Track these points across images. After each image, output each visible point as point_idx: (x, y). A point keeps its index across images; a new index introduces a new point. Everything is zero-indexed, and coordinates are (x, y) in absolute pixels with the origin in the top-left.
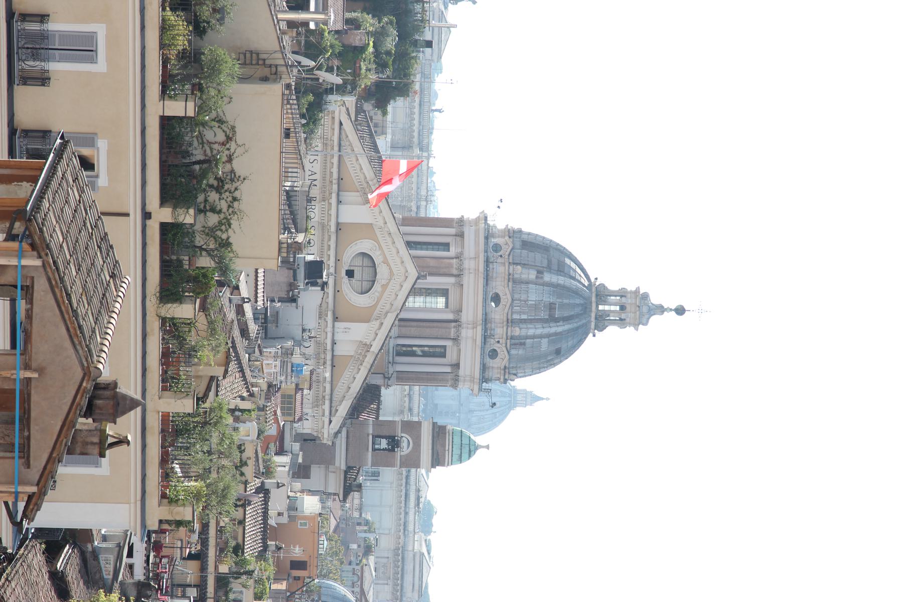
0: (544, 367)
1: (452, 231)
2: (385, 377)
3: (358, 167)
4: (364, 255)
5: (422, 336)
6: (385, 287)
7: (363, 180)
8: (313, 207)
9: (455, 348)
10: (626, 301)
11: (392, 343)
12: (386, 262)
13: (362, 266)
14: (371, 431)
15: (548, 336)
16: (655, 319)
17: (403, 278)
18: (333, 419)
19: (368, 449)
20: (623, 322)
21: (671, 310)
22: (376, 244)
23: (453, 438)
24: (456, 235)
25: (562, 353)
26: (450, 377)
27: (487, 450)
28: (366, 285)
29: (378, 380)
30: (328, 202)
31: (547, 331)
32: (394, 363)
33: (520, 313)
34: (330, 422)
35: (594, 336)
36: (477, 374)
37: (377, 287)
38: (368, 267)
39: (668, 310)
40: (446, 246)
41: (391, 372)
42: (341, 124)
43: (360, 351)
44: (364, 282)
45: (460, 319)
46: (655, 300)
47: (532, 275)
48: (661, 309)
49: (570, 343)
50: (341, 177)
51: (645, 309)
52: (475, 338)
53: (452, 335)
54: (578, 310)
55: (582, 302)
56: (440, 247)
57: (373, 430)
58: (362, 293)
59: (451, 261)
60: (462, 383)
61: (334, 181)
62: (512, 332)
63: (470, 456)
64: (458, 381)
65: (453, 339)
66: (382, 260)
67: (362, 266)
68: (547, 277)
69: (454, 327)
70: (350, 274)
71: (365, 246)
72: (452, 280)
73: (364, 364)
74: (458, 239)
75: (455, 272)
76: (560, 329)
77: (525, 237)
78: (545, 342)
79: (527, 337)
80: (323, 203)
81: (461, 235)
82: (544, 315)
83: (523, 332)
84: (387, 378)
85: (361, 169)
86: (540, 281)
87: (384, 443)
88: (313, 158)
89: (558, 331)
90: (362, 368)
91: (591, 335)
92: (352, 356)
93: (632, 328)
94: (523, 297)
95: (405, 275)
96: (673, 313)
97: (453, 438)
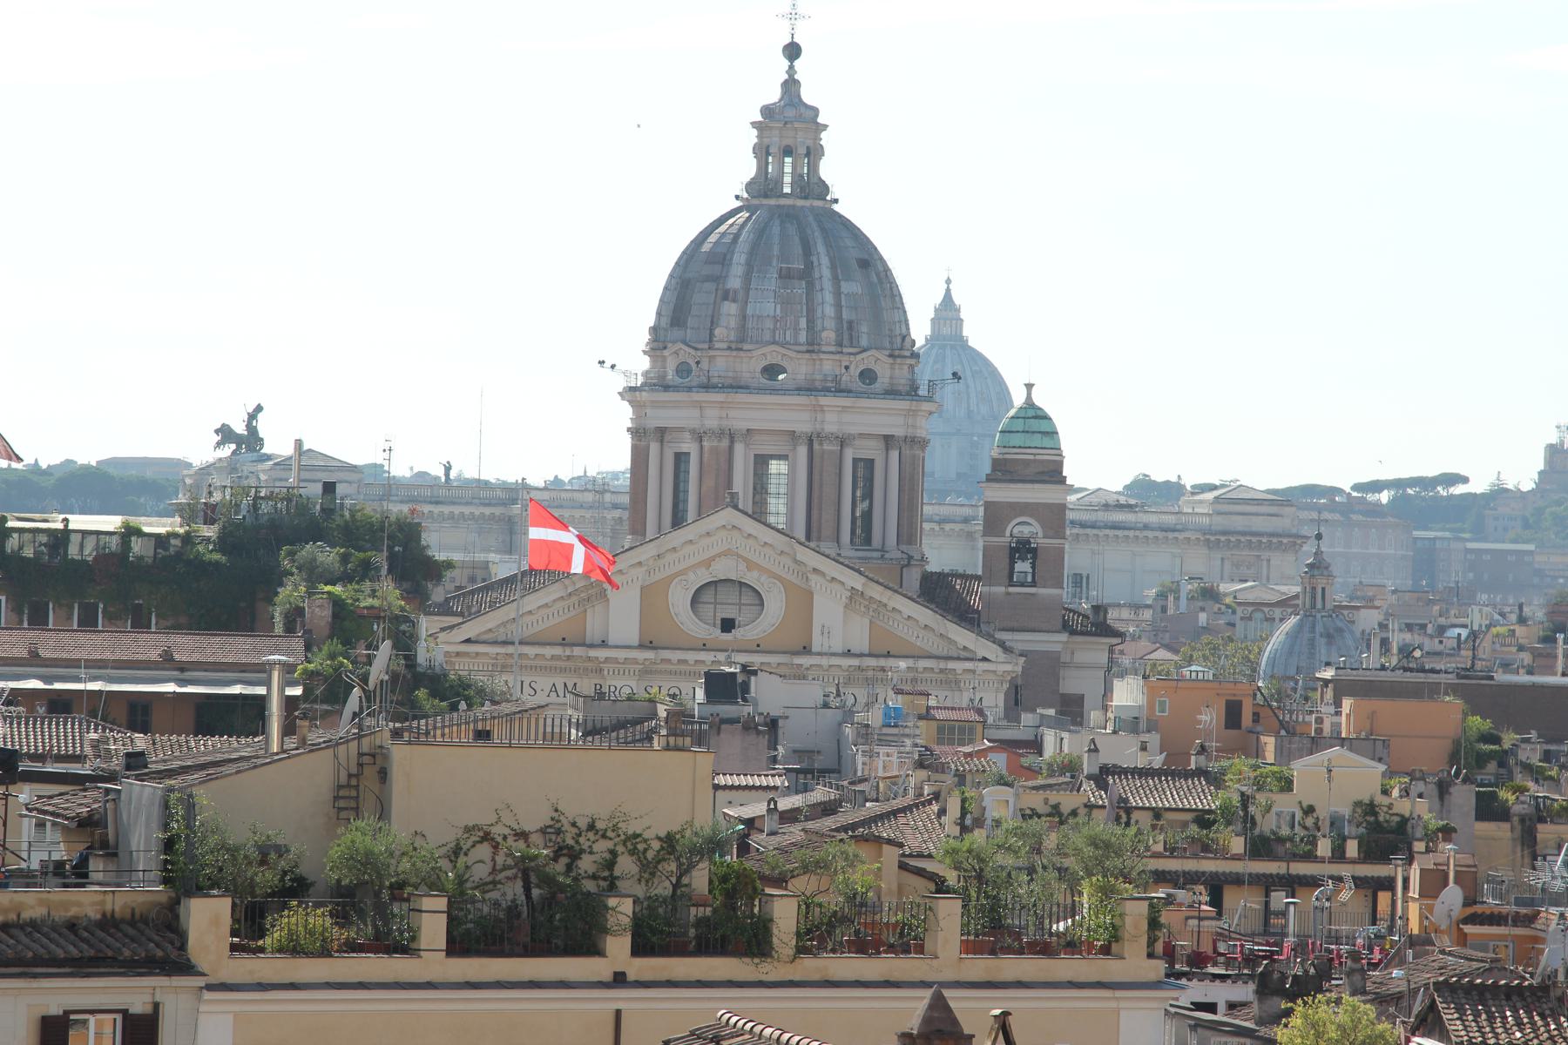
0: (891, 288)
1: (654, 448)
2: (908, 565)
3: (544, 612)
4: (695, 600)
6: (751, 565)
8: (612, 689)
9: (857, 442)
10: (776, 143)
11: (848, 552)
12: (707, 563)
13: (716, 603)
14: (1002, 589)
15: (836, 279)
16: (808, 96)
17: (735, 533)
18: (980, 654)
21: (791, 67)
22: (676, 580)
23: (1014, 447)
24: (662, 442)
25: (866, 257)
26: (907, 452)
27: (1034, 389)
28: (747, 598)
29: (913, 578)
30: (604, 663)
31: (827, 284)
32: (883, 550)
33: (796, 330)
34: (985, 659)
35: (836, 201)
37: (751, 578)
38: (716, 594)
39: (791, 72)
40: (680, 459)
41: (899, 555)
42: (468, 641)
43: (863, 609)
46: (773, 95)
47: (730, 308)
48: (791, 85)
49: (849, 242)
51: (790, 113)
52: (840, 409)
54: (792, 230)
55: (777, 222)
56: (682, 469)
57: (1000, 585)
58: (762, 604)
59: (706, 450)
60: (919, 431)
61: (568, 652)
62: (828, 344)
63: (1046, 417)
64: (915, 437)
65: (841, 446)
66: (703, 569)
67: (716, 603)
68: (735, 282)
69: (821, 444)
70: (728, 625)
71: (679, 599)
72: (739, 448)
73: (885, 600)
74: (667, 437)
75: (725, 443)
76: (825, 261)
77: (665, 321)
78: (846, 287)
79: (839, 318)
80: (606, 672)
81: (661, 433)
82: (800, 288)
83: (830, 323)
84: (909, 562)
86: (741, 295)
87: (1022, 566)
88: (527, 689)
89: (829, 265)
90: (891, 604)
91: (836, 207)
93: (823, 135)
94: (769, 324)
95: (729, 530)
96: (797, 63)
97: (1014, 447)
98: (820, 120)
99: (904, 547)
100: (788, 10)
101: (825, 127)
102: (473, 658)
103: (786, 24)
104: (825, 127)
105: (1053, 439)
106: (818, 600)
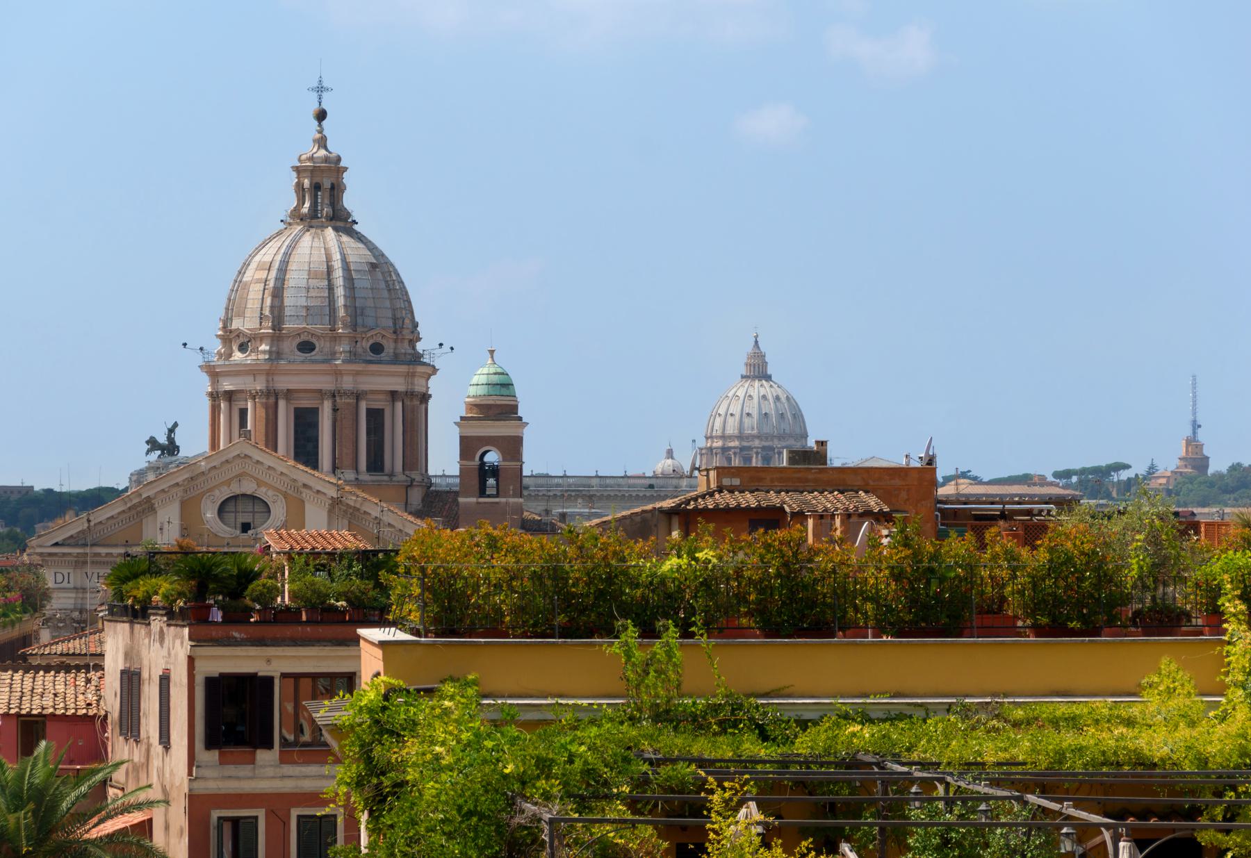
2: (411, 485)
3: (111, 522)
4: (221, 510)
5: (355, 439)
6: (260, 483)
7: (126, 515)
10: (307, 183)
11: (365, 477)
12: (228, 483)
14: (473, 500)
16: (334, 147)
17: (247, 460)
19: (497, 503)
20: (336, 186)
22: (208, 494)
28: (258, 508)
29: (416, 496)
32: (391, 475)
36: (403, 369)
37: (262, 493)
40: (243, 413)
41: (404, 478)
42: (56, 544)
44: (256, 510)
45: (330, 391)
50: (125, 543)
53: (352, 401)
58: (269, 511)
60: (416, 387)
66: (226, 488)
67: (236, 512)
70: (246, 527)
74: (234, 397)
75: (272, 400)
81: (230, 396)
84: (412, 483)
85: (112, 517)
91: (356, 227)
92: (349, 522)
93: (345, 175)
95: (242, 458)
96: (324, 123)
98: (342, 164)
99: (407, 472)
100: (316, 84)
101: (346, 169)
102: (60, 557)
103: (315, 95)
104: (346, 169)
105: (508, 389)
106: (308, 506)
